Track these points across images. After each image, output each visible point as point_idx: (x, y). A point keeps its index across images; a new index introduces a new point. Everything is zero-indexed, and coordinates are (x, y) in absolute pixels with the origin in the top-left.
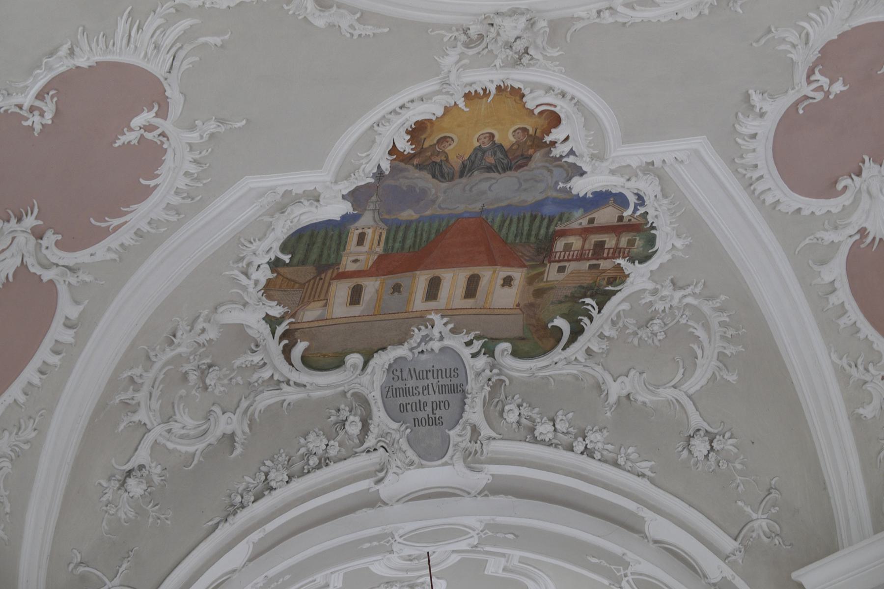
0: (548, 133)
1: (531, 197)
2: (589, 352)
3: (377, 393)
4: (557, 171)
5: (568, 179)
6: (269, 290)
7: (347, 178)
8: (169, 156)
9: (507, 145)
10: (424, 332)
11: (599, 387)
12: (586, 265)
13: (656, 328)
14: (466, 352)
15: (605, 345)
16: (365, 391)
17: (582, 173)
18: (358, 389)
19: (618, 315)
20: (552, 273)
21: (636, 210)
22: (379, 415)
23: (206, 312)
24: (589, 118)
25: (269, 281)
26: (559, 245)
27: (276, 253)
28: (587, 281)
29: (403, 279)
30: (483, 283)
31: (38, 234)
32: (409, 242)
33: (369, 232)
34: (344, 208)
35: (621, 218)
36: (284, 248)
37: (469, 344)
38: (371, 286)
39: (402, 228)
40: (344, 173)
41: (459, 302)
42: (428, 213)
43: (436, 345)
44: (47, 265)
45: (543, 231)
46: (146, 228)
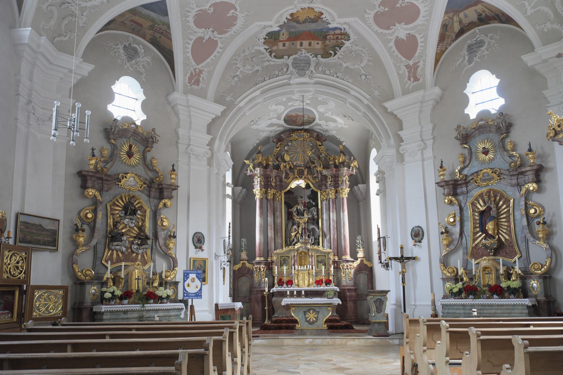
0: (321, 16)
1: (320, 28)
2: (339, 58)
3: (291, 64)
4: (324, 23)
5: (328, 25)
6: (264, 43)
7: (278, 23)
8: (238, 18)
9: (312, 18)
10: (301, 52)
11: (341, 65)
12: (335, 41)
13: (353, 54)
14: (311, 57)
15: (342, 57)
16: (288, 63)
17: (330, 24)
18: (287, 62)
19: (344, 51)
20: (327, 42)
21: (344, 31)
22: (291, 68)
23: (251, 47)
24: (330, 14)
25: (264, 42)
26: (328, 37)
27: (265, 36)
28: (336, 44)
29: (294, 42)
30: (312, 44)
31: (213, 32)
32: (294, 35)
33: (285, 33)
34: (279, 29)
35: (341, 32)
36: (266, 35)
37: (311, 55)
38: (287, 44)
39: (292, 34)
40: (277, 22)
41: (307, 47)
42: (297, 30)
43: (304, 55)
44: (216, 37)
45: (324, 34)
46: (236, 31)
